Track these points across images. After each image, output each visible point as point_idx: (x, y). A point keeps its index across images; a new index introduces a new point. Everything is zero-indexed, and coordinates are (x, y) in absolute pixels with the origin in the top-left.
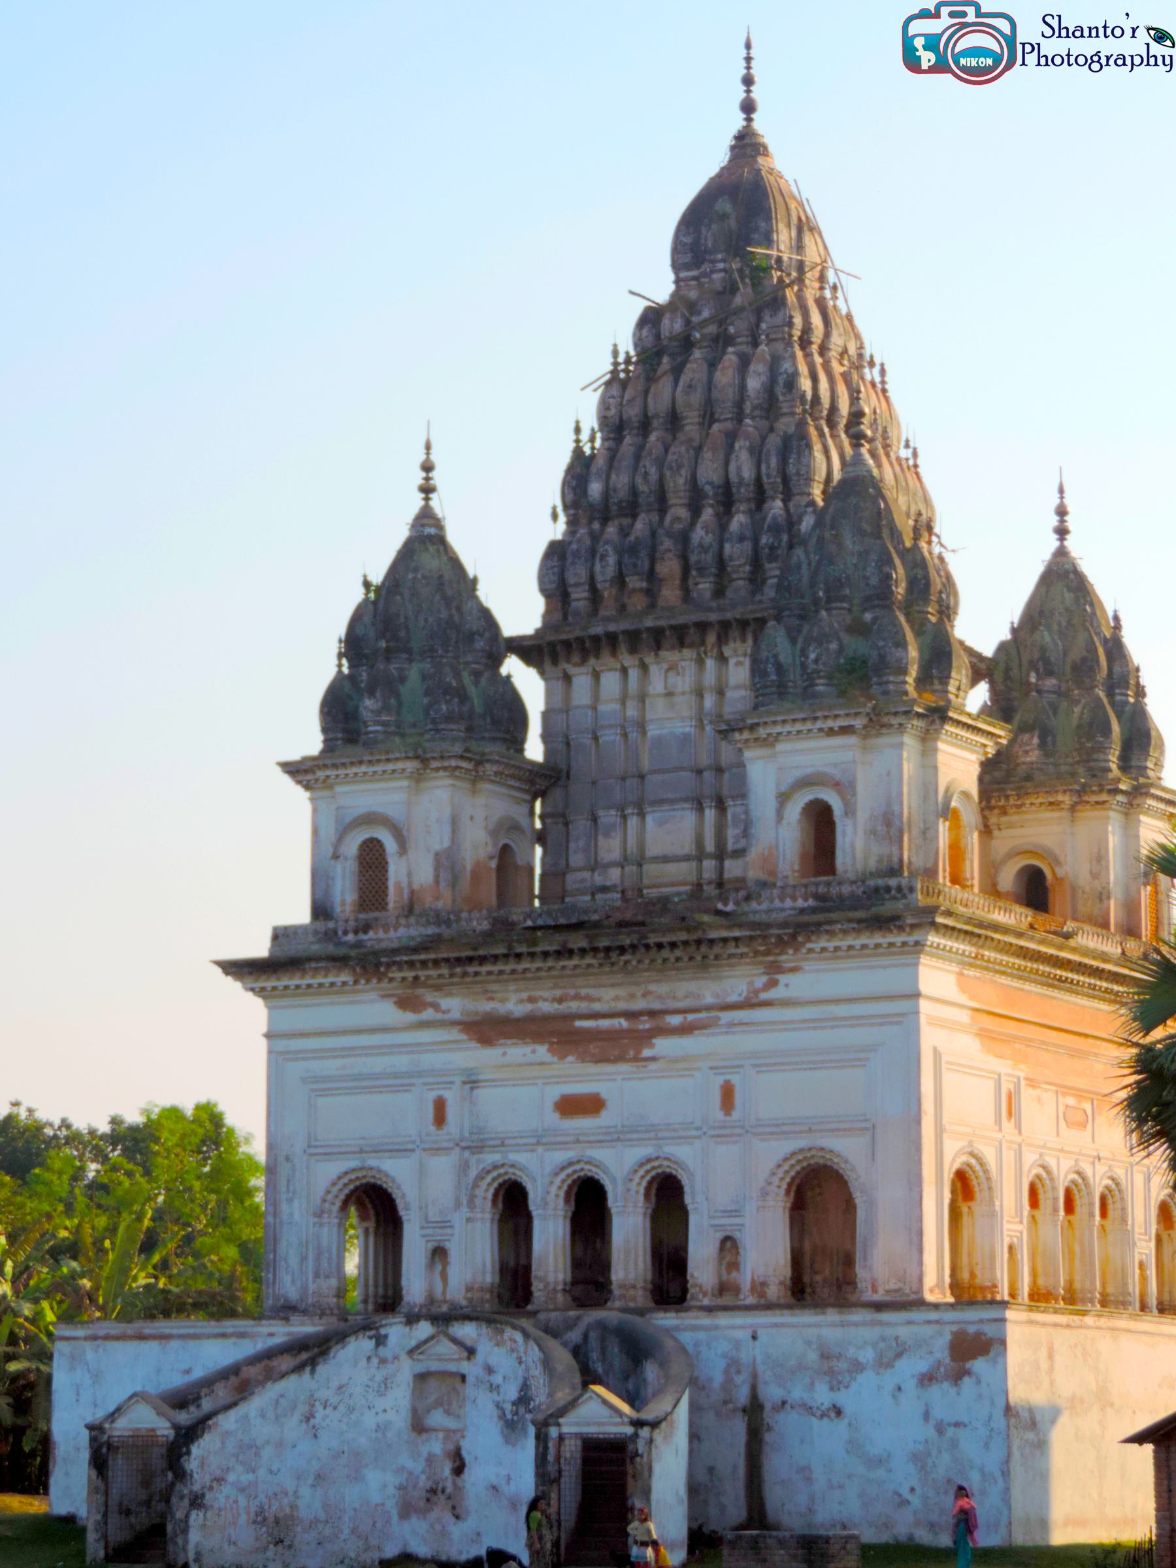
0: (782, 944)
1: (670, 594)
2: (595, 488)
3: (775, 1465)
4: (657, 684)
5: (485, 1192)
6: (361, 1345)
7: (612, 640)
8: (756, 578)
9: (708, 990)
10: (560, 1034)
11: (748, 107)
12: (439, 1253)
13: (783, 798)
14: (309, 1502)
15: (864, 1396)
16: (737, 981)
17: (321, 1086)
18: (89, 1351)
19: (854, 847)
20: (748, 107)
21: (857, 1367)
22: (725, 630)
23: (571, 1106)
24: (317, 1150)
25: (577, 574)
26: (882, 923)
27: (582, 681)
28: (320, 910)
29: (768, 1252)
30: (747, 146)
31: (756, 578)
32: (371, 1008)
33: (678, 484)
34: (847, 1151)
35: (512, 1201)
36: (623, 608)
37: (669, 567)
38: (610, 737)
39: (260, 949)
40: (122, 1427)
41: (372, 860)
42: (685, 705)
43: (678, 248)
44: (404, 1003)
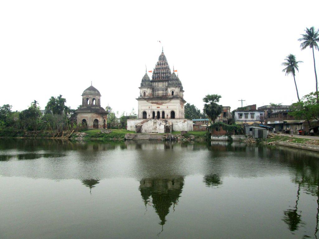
0: (171, 99)
1: (161, 78)
2: (155, 72)
3: (173, 127)
4: (160, 83)
5: (152, 112)
6: (150, 121)
7: (157, 81)
8: (166, 78)
9: (166, 101)
10: (157, 103)
11: (163, 51)
12: (149, 115)
13: (171, 91)
14: (147, 129)
15: (178, 124)
16: (168, 101)
17: (142, 106)
18: (130, 121)
19: (175, 94)
20: (163, 51)
21: (178, 122)
22: (164, 81)
23: (158, 107)
24: (141, 110)
25: (154, 77)
26: (177, 98)
27: (155, 83)
28: (141, 96)
29: (169, 116)
30: (163, 53)
31: (166, 78)
32: (145, 102)
33: (161, 72)
34: (175, 111)
35: (154, 113)
36: (157, 79)
37: (161, 77)
38: (157, 86)
39: (138, 98)
40: (138, 125)
41: (145, 93)
42: (161, 85)
43: (159, 58)
44: (147, 101)
